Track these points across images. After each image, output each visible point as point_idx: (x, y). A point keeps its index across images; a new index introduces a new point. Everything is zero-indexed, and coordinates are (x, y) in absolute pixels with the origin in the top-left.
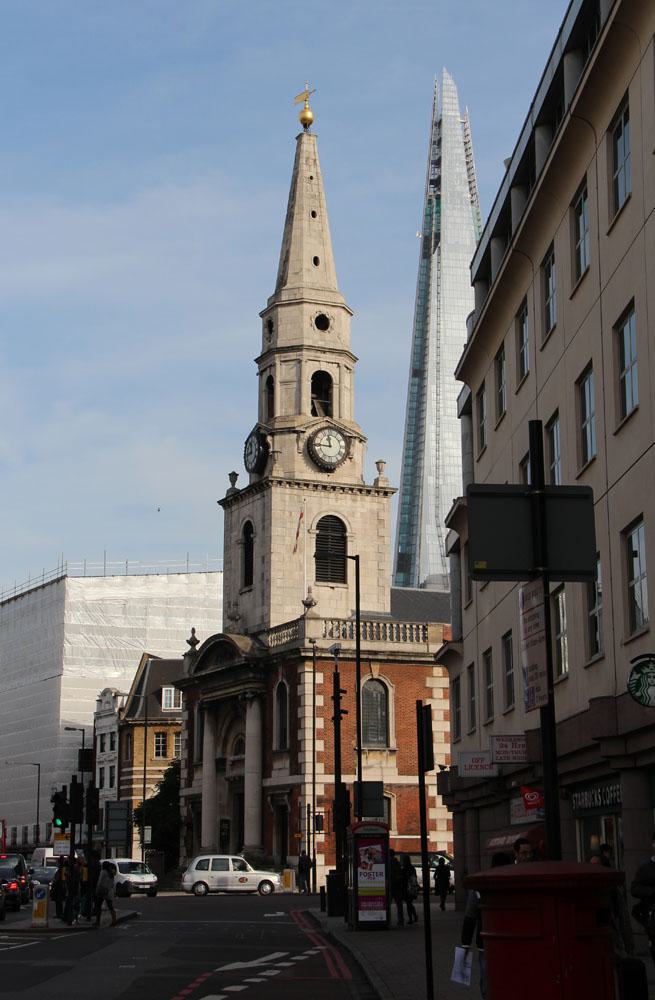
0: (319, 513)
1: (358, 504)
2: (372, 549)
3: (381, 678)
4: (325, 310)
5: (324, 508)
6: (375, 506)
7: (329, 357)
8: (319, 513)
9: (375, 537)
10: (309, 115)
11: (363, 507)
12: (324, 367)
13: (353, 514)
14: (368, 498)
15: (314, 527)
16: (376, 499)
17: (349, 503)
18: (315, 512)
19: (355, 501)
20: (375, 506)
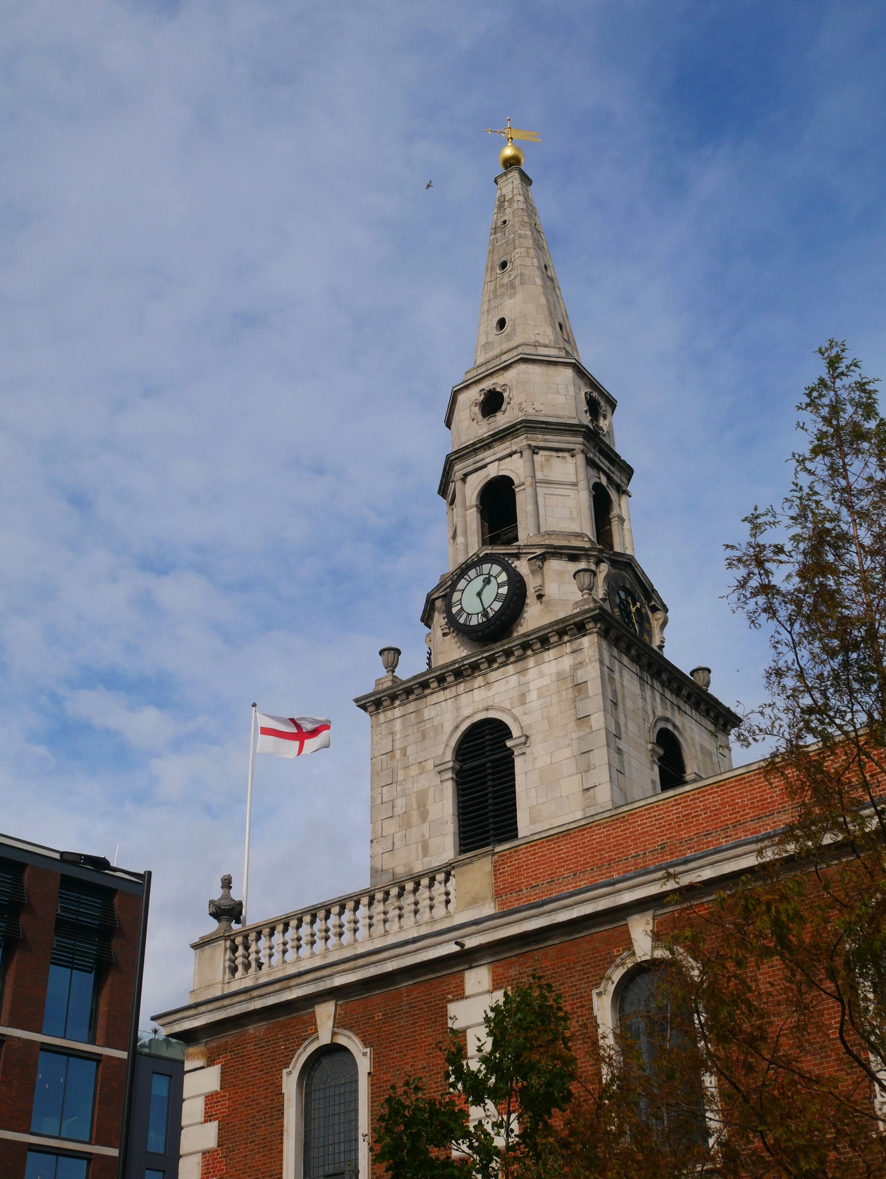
0: (457, 727)
1: (532, 673)
2: (567, 752)
3: (342, 1040)
4: (487, 385)
5: (466, 712)
6: (567, 662)
7: (501, 449)
8: (457, 727)
9: (572, 725)
10: (508, 152)
11: (542, 675)
12: (493, 471)
13: (523, 698)
14: (550, 654)
15: (449, 756)
16: (568, 648)
17: (514, 680)
18: (448, 727)
19: (523, 672)
20: (567, 662)
